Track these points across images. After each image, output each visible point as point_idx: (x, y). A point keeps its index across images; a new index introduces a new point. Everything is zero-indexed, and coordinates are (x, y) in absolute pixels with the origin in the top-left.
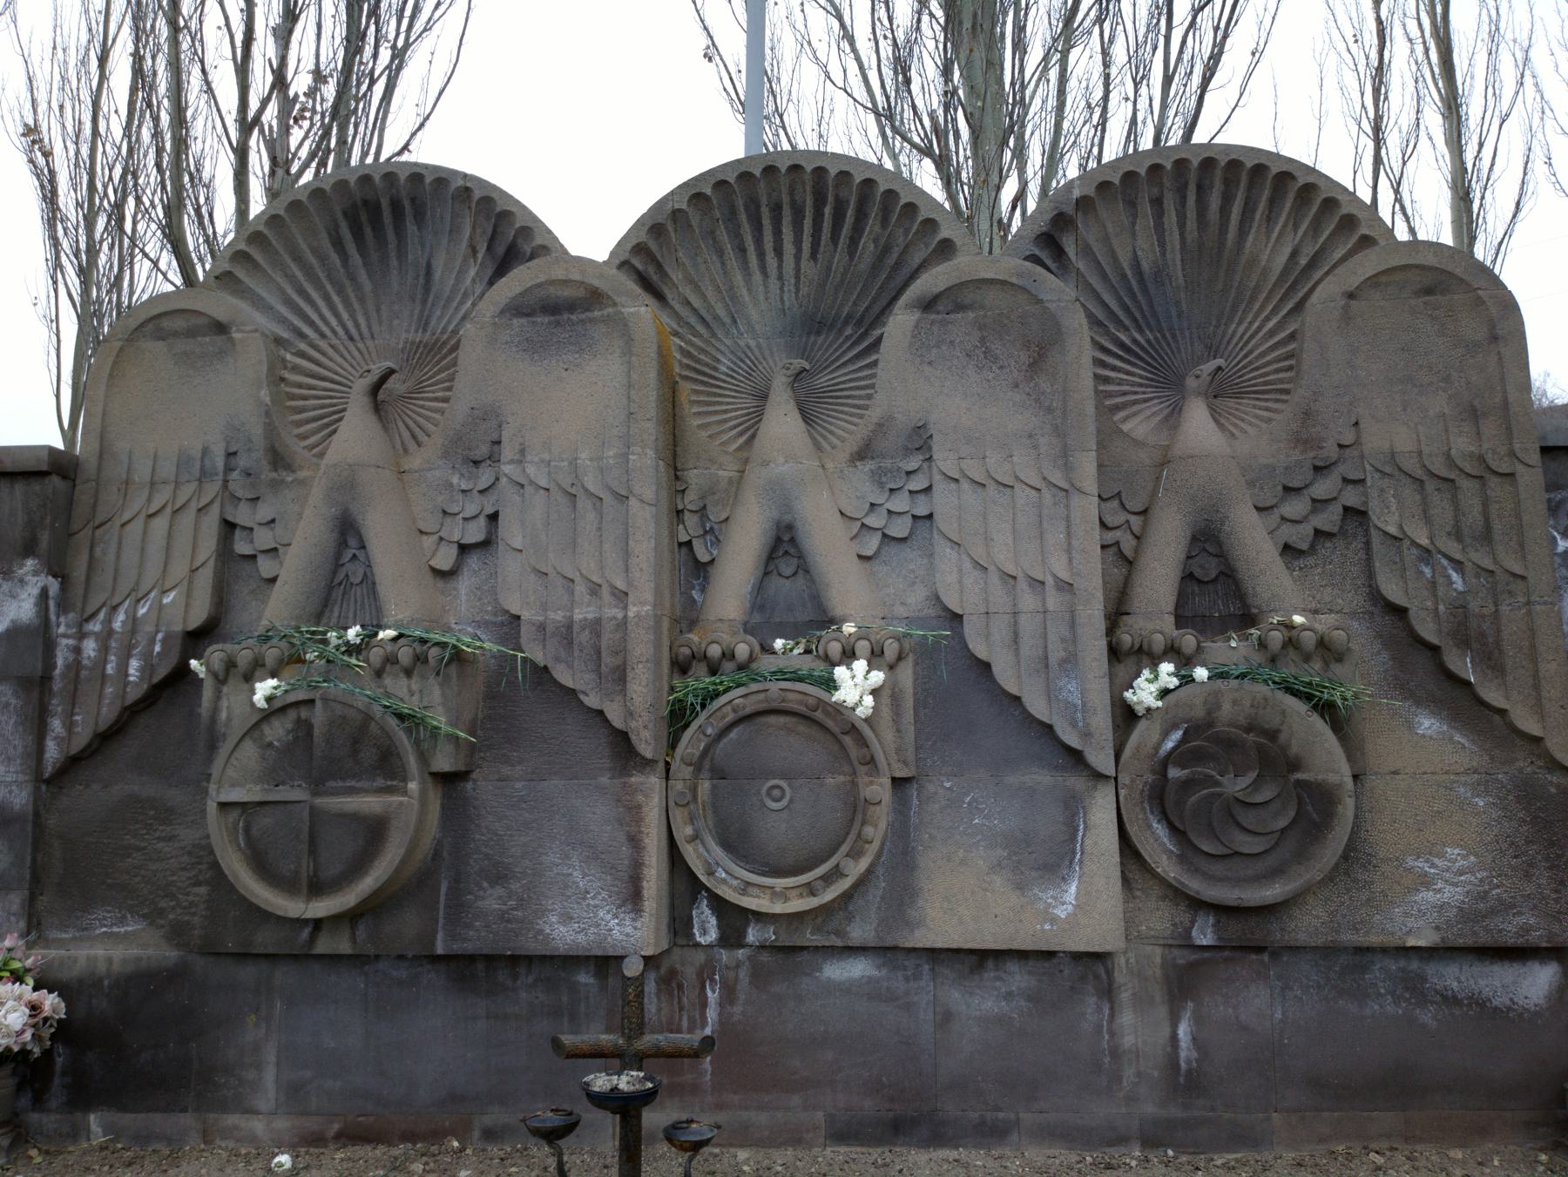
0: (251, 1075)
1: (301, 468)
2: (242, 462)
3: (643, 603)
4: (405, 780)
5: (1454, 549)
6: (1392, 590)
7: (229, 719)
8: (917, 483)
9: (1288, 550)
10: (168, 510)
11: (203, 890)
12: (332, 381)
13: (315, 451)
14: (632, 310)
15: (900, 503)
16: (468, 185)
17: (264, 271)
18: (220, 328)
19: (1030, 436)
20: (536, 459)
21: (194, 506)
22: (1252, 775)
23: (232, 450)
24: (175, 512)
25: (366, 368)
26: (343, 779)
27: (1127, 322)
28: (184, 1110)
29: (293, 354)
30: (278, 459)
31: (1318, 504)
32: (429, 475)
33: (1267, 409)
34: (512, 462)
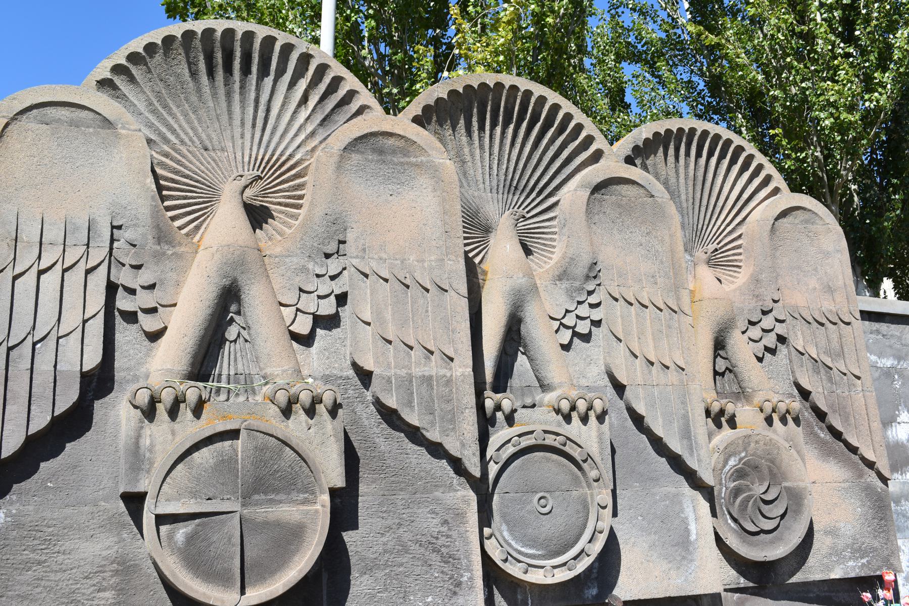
1: (180, 244)
3: (466, 366)
4: (313, 493)
7: (152, 445)
8: (593, 300)
10: (58, 268)
11: (107, 594)
12: (191, 179)
14: (441, 161)
15: (584, 311)
16: (311, 52)
18: (107, 123)
19: (653, 277)
20: (376, 257)
22: (766, 484)
23: (115, 224)
24: (65, 271)
25: (241, 173)
26: (265, 493)
29: (157, 152)
33: (730, 276)
34: (357, 257)
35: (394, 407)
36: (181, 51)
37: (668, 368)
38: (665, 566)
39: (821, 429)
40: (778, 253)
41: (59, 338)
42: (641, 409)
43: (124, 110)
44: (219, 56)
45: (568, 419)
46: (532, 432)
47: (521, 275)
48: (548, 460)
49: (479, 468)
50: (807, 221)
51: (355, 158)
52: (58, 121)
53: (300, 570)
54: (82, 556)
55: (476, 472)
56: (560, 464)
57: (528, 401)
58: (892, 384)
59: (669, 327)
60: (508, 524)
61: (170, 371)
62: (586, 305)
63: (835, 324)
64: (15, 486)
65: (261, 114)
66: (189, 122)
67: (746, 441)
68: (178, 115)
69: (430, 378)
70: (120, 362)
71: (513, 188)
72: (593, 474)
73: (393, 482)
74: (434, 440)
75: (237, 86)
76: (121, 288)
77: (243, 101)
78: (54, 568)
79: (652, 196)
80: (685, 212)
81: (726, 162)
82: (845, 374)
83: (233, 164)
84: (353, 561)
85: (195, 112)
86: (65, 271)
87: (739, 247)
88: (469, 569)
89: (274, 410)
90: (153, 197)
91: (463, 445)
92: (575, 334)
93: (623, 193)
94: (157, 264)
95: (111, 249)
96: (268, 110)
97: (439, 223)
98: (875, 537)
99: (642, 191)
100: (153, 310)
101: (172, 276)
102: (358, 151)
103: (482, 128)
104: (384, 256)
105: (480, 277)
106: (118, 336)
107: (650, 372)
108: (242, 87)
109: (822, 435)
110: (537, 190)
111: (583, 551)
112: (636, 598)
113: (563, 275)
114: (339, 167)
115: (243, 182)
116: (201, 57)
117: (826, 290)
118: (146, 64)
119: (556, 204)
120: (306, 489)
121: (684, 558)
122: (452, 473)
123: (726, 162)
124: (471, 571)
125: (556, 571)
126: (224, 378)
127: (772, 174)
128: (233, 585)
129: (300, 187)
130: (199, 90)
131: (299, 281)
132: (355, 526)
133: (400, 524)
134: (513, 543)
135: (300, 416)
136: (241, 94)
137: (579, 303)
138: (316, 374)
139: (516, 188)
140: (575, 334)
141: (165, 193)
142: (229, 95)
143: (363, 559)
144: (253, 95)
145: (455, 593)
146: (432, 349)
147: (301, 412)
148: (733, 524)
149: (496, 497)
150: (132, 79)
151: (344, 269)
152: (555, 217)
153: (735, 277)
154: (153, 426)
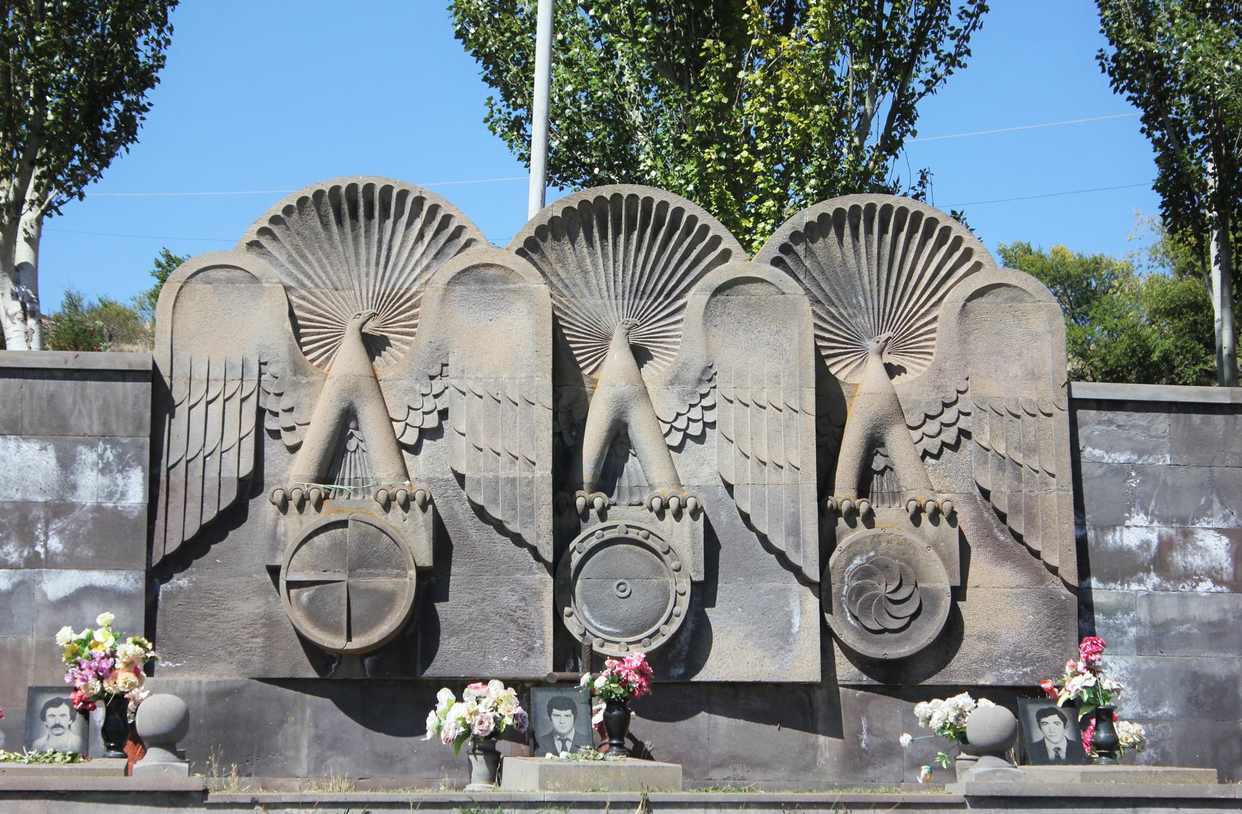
0: (291, 753)
2: (270, 370)
3: (546, 469)
4: (404, 569)
5: (1019, 458)
7: (286, 532)
8: (707, 402)
10: (221, 399)
11: (258, 640)
13: (315, 363)
15: (696, 413)
16: (423, 195)
17: (279, 240)
18: (254, 279)
19: (776, 377)
20: (473, 377)
21: (238, 397)
22: (897, 583)
24: (225, 401)
26: (367, 568)
27: (836, 301)
28: (249, 775)
32: (398, 383)
33: (919, 364)
35: (482, 504)
36: (313, 208)
37: (782, 467)
38: (759, 653)
39: (1002, 531)
40: (972, 337)
41: (222, 453)
42: (747, 509)
43: (268, 266)
44: (345, 207)
46: (615, 527)
47: (624, 383)
48: (630, 551)
49: (552, 555)
50: (1013, 300)
51: (459, 289)
52: (219, 280)
53: (391, 626)
54: (241, 612)
55: (549, 558)
56: (641, 555)
57: (636, 500)
58: (1125, 481)
59: (787, 427)
60: (588, 606)
61: (301, 476)
62: (699, 408)
63: (1034, 416)
64: (195, 562)
65: (384, 253)
66: (323, 267)
67: (876, 540)
68: (314, 262)
69: (514, 479)
70: (268, 470)
71: (640, 293)
72: (674, 565)
73: (481, 565)
74: (515, 531)
75: (362, 230)
76: (267, 412)
77: (368, 244)
78: (222, 620)
79: (783, 293)
80: (869, 295)
81: (918, 236)
82: (1037, 472)
83: (359, 300)
84: (443, 626)
85: (327, 257)
86: (225, 401)
87: (933, 331)
88: (541, 637)
89: (377, 506)
90: (290, 338)
91: (538, 536)
92: (686, 436)
93: (752, 292)
94: (294, 391)
95: (259, 381)
96: (390, 249)
97: (531, 343)
98: (1047, 646)
99: (772, 289)
100: (292, 429)
101: (307, 400)
102: (462, 283)
103: (604, 237)
104: (480, 375)
105: (587, 385)
106: (267, 450)
107: (762, 472)
108: (367, 231)
109: (1002, 538)
110: (665, 293)
111: (658, 631)
112: (724, 680)
113: (674, 380)
114: (443, 299)
115: (361, 320)
116: (331, 211)
117: (1029, 377)
118: (285, 224)
119: (684, 306)
120: (398, 566)
121: (781, 648)
122: (532, 559)
123: (918, 236)
124: (543, 639)
125: (630, 647)
126: (346, 481)
127: (972, 247)
128: (342, 634)
129: (414, 317)
130: (330, 238)
131: (408, 400)
132: (446, 599)
133: (484, 599)
134: (593, 621)
135: (397, 510)
136: (366, 237)
137: (691, 406)
138: (422, 477)
139: (643, 292)
140: (686, 436)
141: (302, 331)
142: (356, 239)
143: (451, 625)
144: (376, 237)
145: (528, 656)
146: (517, 455)
147: (399, 507)
148: (852, 622)
149: (579, 582)
150: (274, 237)
151: (447, 388)
152: (682, 320)
153: (924, 365)
154: (286, 517)
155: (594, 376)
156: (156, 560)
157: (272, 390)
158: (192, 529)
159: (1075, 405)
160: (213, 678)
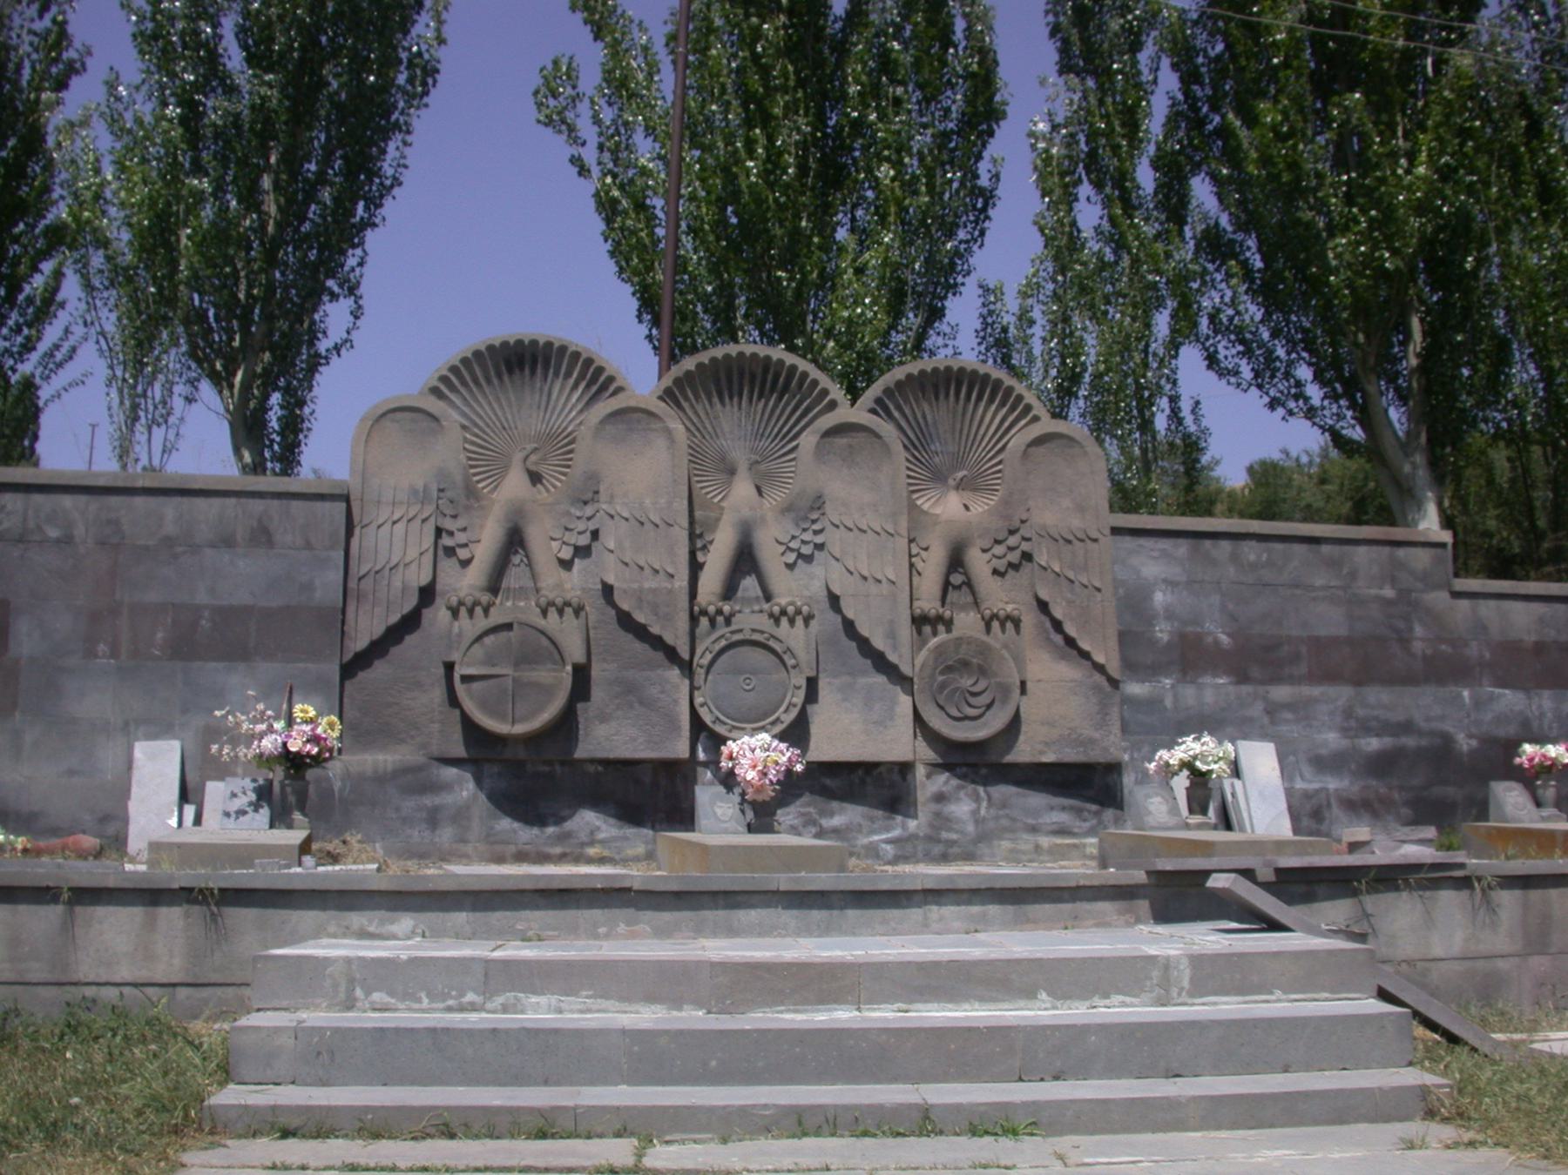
2: (449, 494)
5: (1071, 575)
6: (1043, 595)
8: (816, 527)
9: (995, 572)
11: (437, 726)
15: (807, 536)
18: (435, 418)
30: (471, 492)
31: (1011, 549)
45: (777, 621)
55: (686, 656)
66: (493, 409)
100: (466, 545)
113: (788, 509)
115: (525, 453)
119: (796, 447)
129: (571, 452)
135: (553, 614)
137: (805, 530)
140: (800, 556)
155: (724, 504)
156: (348, 656)
157: (447, 512)
158: (378, 630)
159: (1116, 531)
160: (397, 757)
